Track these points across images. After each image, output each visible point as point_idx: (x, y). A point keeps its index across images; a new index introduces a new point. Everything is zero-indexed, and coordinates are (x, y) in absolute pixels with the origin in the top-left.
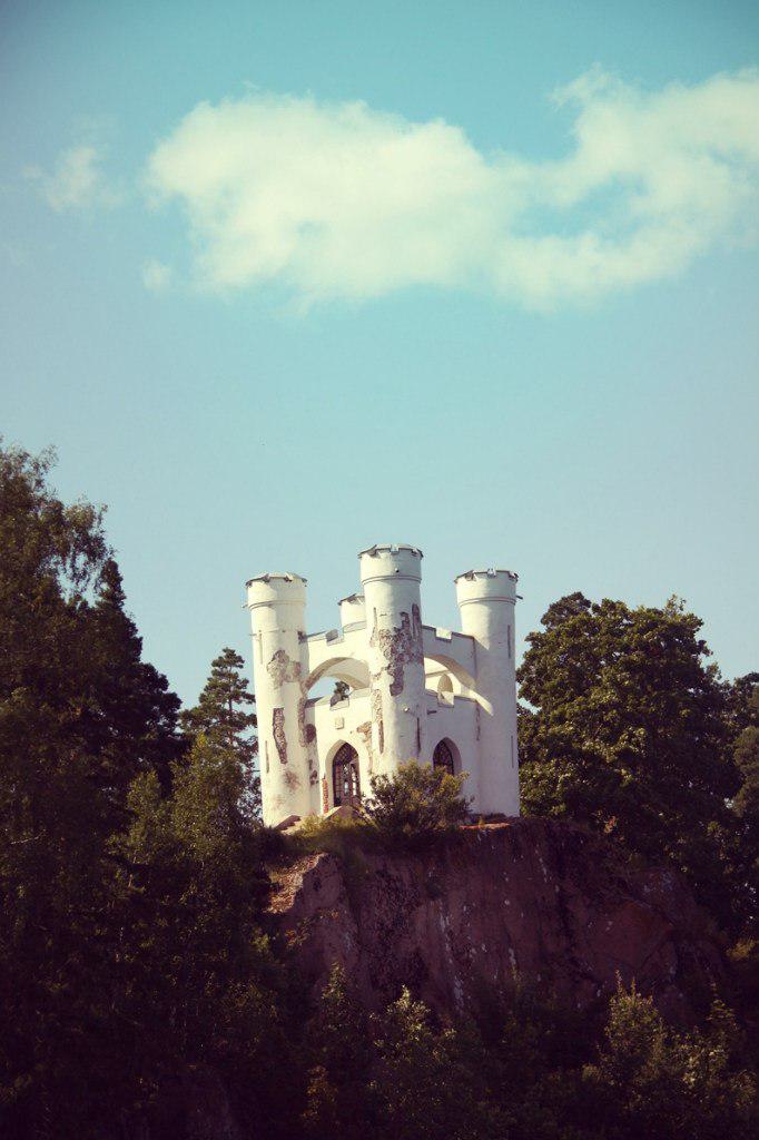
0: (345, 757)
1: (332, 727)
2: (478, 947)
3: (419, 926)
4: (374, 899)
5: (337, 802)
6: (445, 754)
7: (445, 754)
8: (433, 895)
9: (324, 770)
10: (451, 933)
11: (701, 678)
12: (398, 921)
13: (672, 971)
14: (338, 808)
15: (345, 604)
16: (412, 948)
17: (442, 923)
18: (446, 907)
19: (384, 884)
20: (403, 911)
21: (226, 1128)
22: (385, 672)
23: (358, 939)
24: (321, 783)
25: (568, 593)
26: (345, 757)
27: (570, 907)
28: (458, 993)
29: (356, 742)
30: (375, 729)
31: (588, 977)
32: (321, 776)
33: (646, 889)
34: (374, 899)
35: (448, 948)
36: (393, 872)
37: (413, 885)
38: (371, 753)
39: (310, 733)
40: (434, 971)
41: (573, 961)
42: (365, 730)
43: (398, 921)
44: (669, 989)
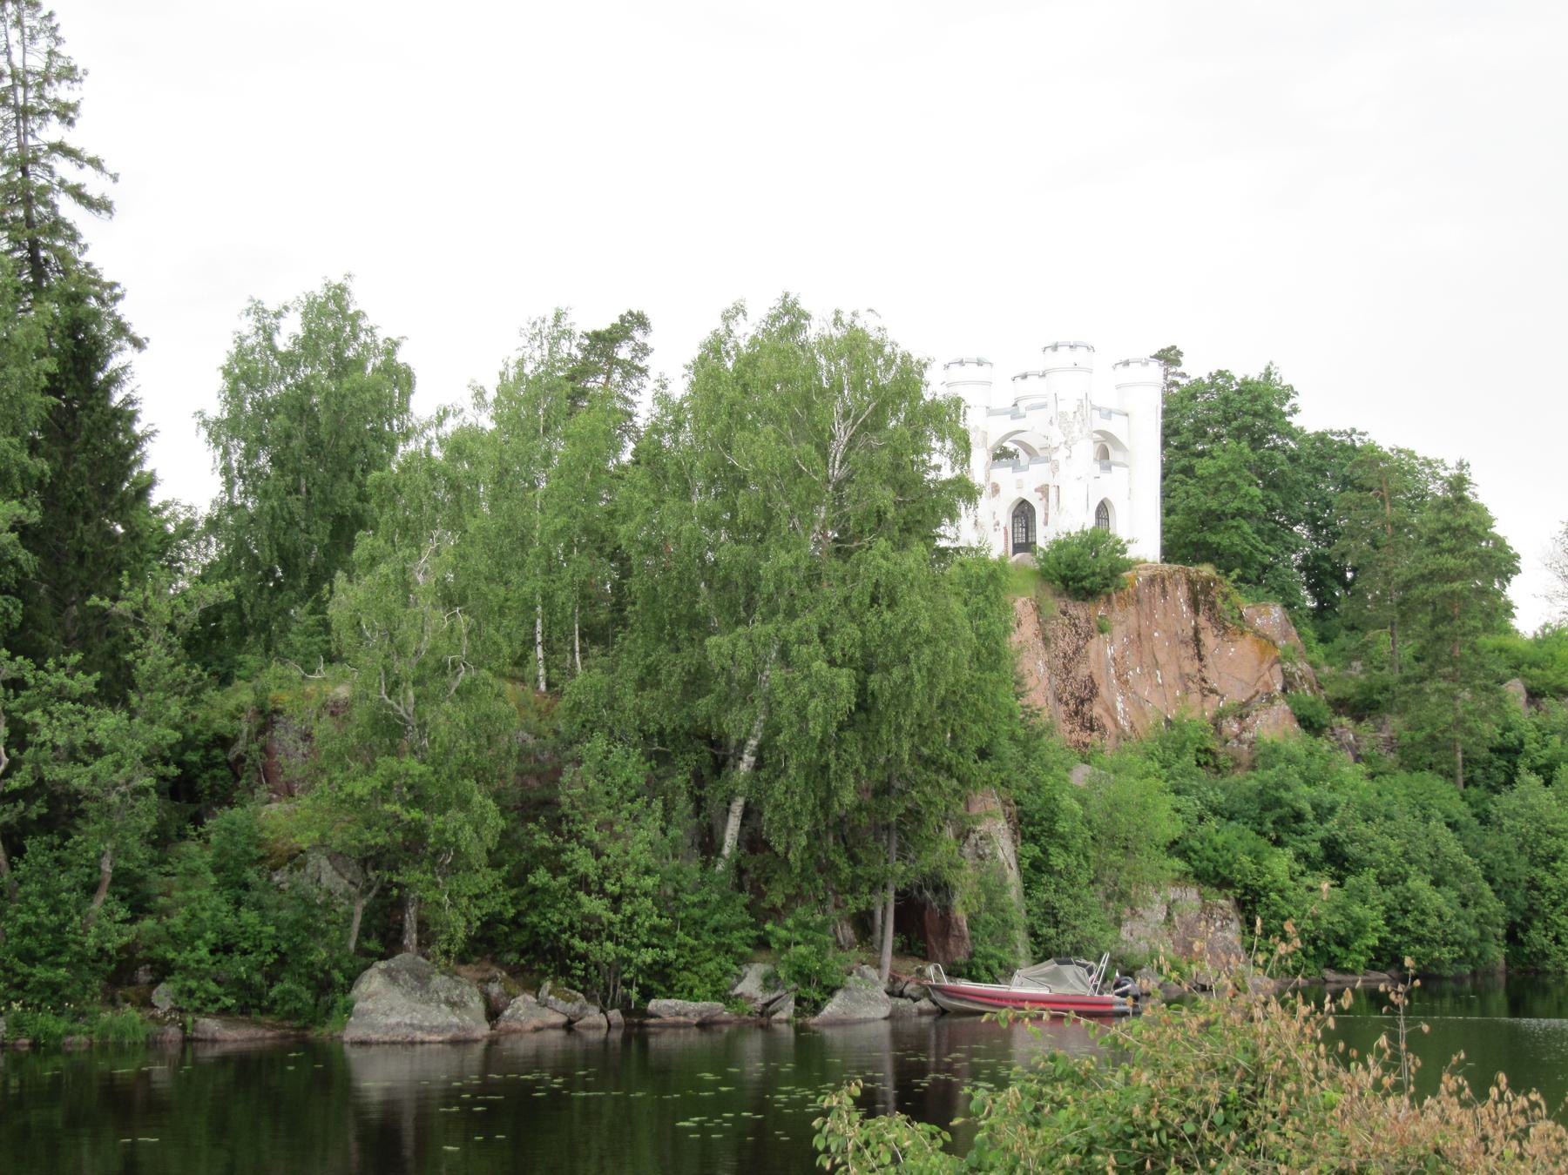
0: (1023, 513)
1: (1013, 484)
2: (1134, 670)
3: (1092, 654)
4: (1060, 634)
5: (1018, 548)
6: (1103, 510)
7: (1103, 510)
8: (1102, 632)
9: (1005, 519)
10: (1114, 659)
11: (1291, 433)
12: (1077, 650)
13: (1279, 687)
14: (1018, 555)
15: (1018, 379)
16: (1087, 672)
18: (1112, 640)
19: (1067, 622)
20: (1081, 643)
21: (999, 826)
22: (1062, 447)
23: (1048, 664)
24: (1002, 531)
25: (1165, 347)
26: (1023, 513)
27: (1202, 636)
28: (1119, 706)
29: (1034, 499)
30: (1052, 493)
31: (1212, 691)
32: (1002, 525)
34: (1060, 634)
35: (1112, 671)
36: (1072, 611)
37: (1088, 621)
38: (1047, 508)
39: (996, 490)
40: (1103, 690)
41: (1204, 680)
42: (1043, 490)
43: (1077, 650)
44: (1277, 702)
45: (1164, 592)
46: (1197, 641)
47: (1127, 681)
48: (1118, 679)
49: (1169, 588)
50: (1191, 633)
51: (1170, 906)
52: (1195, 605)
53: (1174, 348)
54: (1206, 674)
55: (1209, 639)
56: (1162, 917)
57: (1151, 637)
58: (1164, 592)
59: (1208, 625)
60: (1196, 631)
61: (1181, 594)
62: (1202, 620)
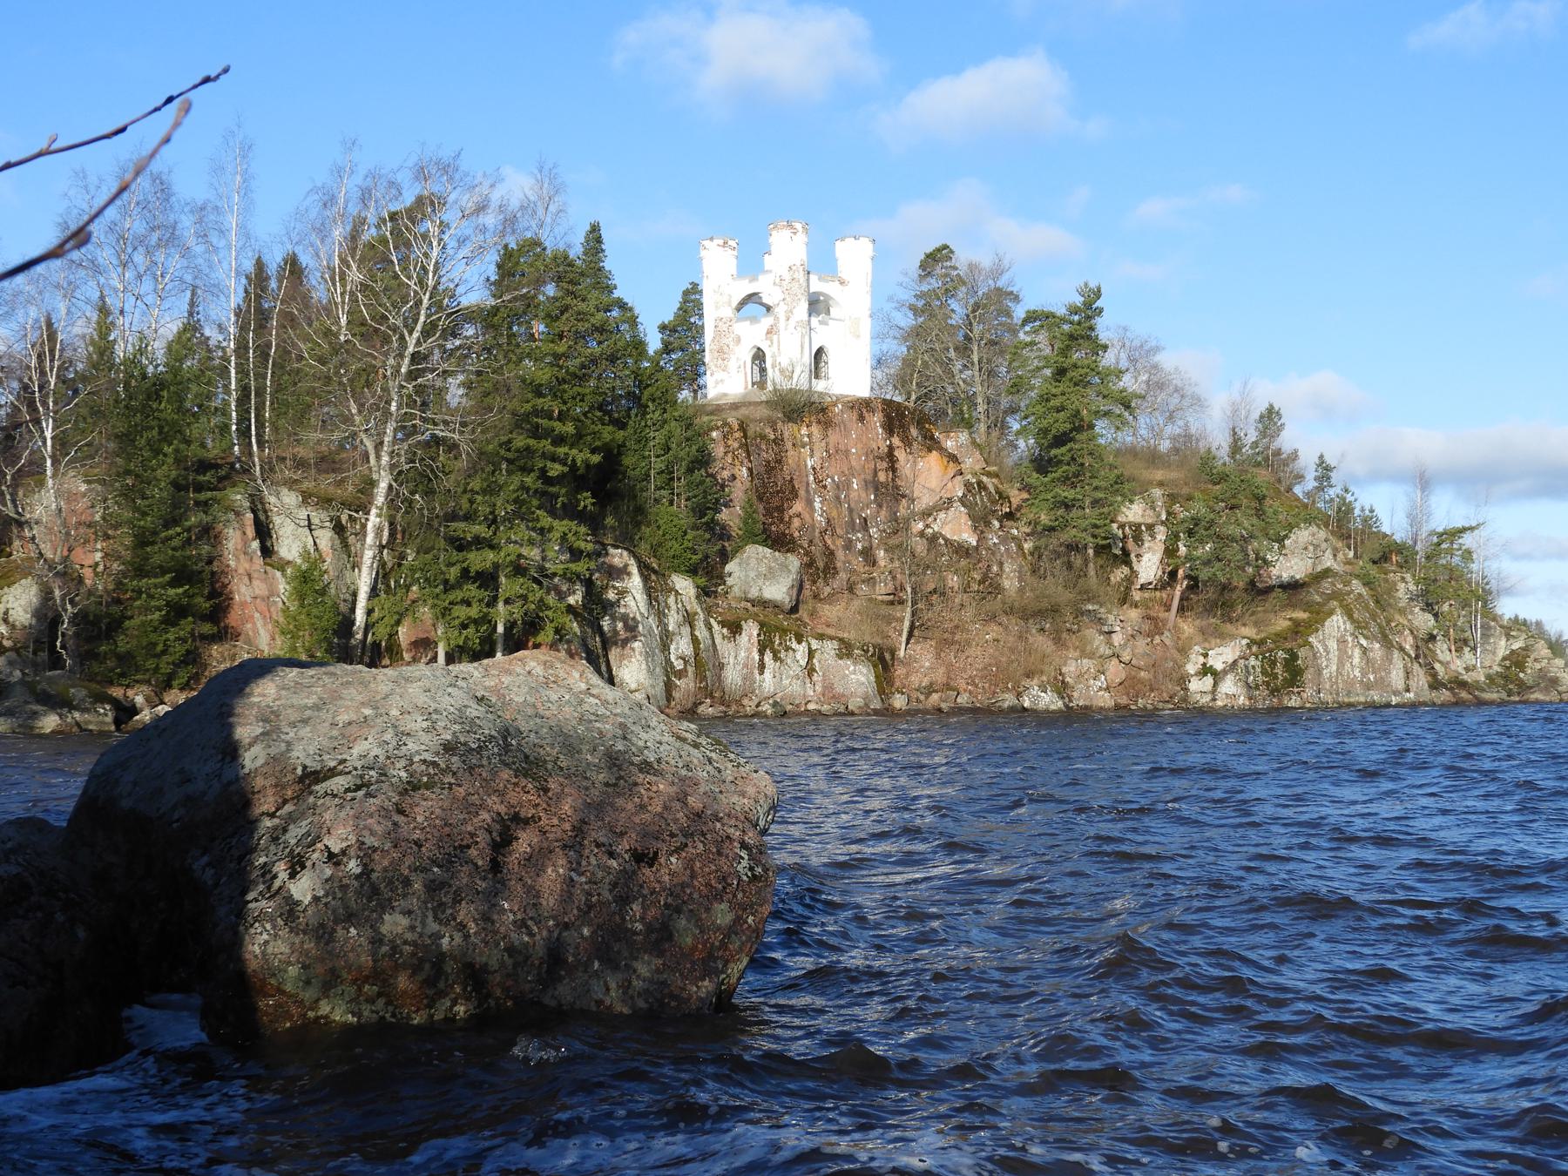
0: (759, 356)
10: (814, 469)
17: (809, 463)
26: (759, 356)
27: (896, 453)
28: (817, 505)
33: (949, 443)
35: (812, 478)
39: (738, 340)
40: (802, 493)
45: (861, 418)
46: (890, 456)
47: (825, 487)
48: (818, 482)
49: (866, 415)
50: (886, 450)
51: (811, 653)
52: (889, 428)
53: (946, 247)
54: (899, 483)
55: (900, 454)
56: (803, 663)
57: (847, 452)
58: (861, 418)
59: (901, 444)
60: (891, 448)
61: (876, 420)
62: (896, 441)
